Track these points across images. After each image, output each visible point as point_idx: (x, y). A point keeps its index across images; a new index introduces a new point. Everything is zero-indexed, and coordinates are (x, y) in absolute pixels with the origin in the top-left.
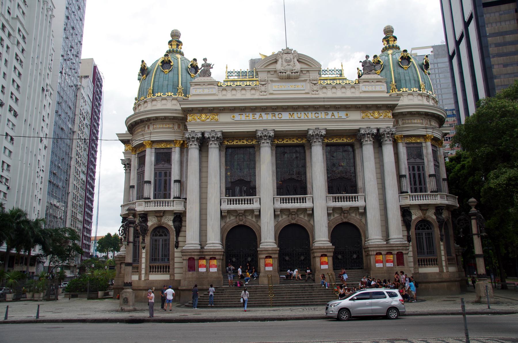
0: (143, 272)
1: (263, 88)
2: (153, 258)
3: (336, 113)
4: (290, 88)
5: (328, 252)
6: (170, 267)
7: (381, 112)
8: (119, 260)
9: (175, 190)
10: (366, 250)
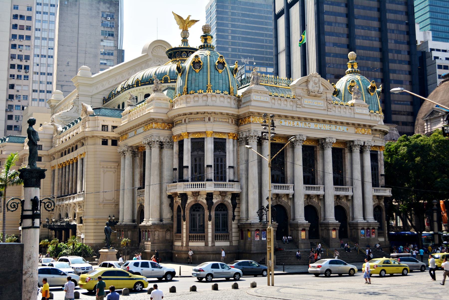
0: (210, 239)
1: (299, 102)
2: (217, 228)
3: (341, 127)
4: (315, 104)
5: (337, 226)
6: (230, 236)
7: (366, 129)
8: (154, 228)
9: (230, 174)
10: (351, 225)
